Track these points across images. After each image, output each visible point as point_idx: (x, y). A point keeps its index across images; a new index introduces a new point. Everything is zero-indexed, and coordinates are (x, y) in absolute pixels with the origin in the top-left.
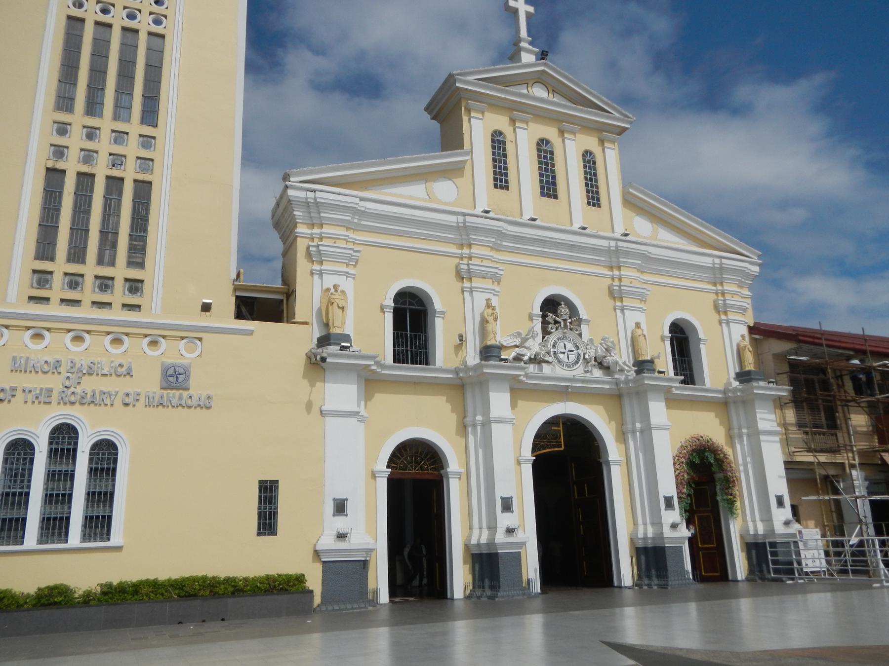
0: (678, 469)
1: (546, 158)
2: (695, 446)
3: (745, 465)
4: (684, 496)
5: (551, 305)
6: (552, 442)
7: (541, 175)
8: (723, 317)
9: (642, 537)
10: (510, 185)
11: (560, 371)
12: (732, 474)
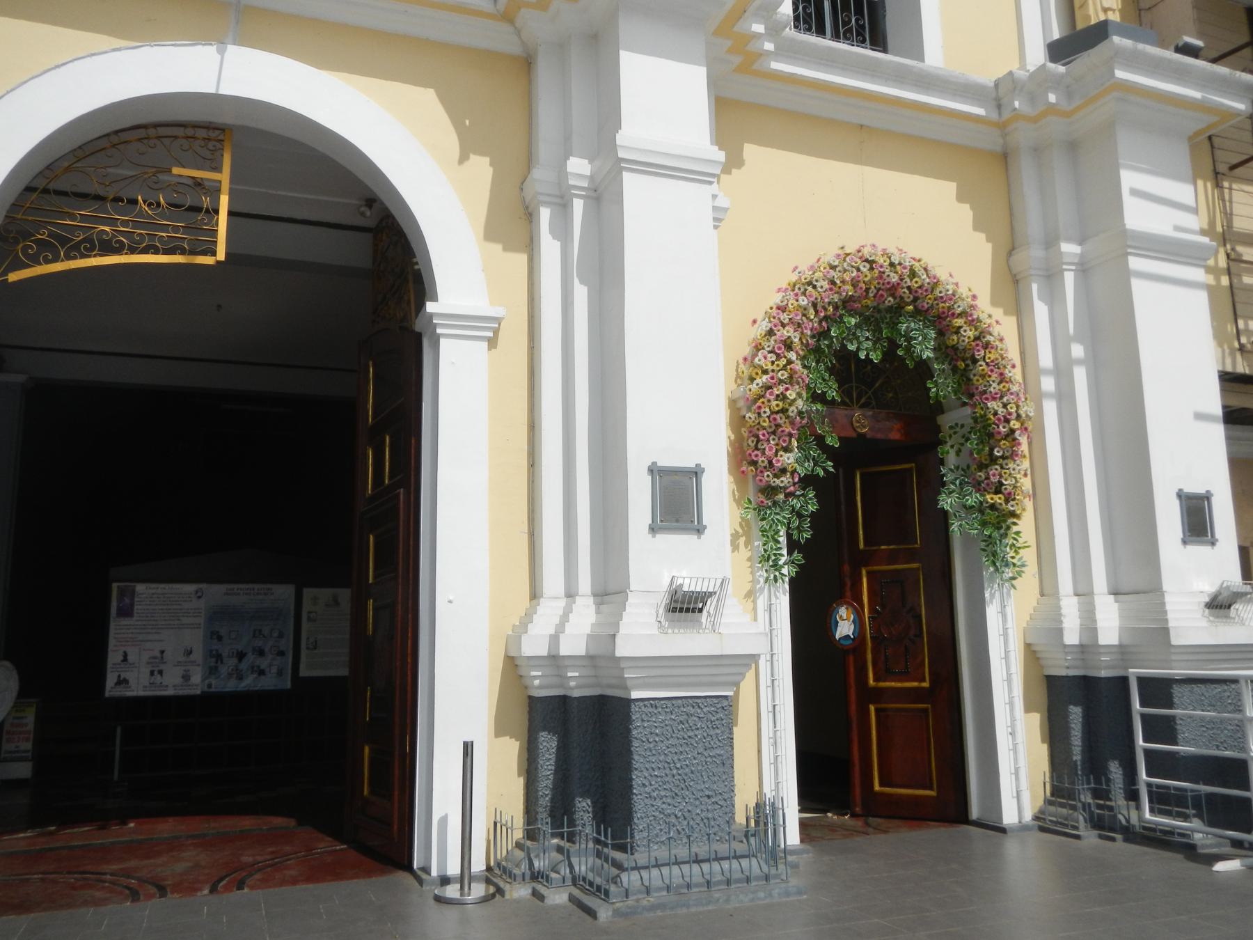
0: (765, 372)
2: (854, 284)
3: (1062, 372)
4: (785, 480)
6: (164, 228)
9: (580, 650)
12: (1005, 406)
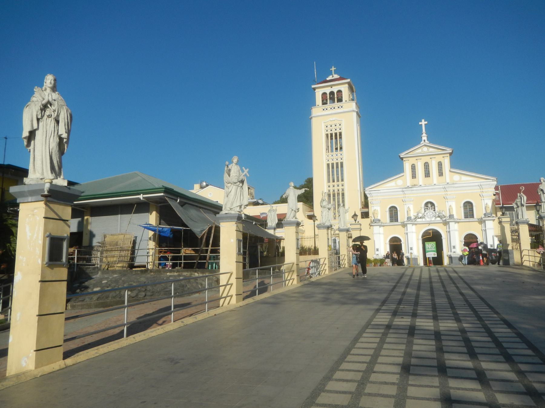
1: (427, 167)
5: (426, 204)
7: (425, 172)
8: (482, 199)
10: (416, 177)
11: (428, 219)
